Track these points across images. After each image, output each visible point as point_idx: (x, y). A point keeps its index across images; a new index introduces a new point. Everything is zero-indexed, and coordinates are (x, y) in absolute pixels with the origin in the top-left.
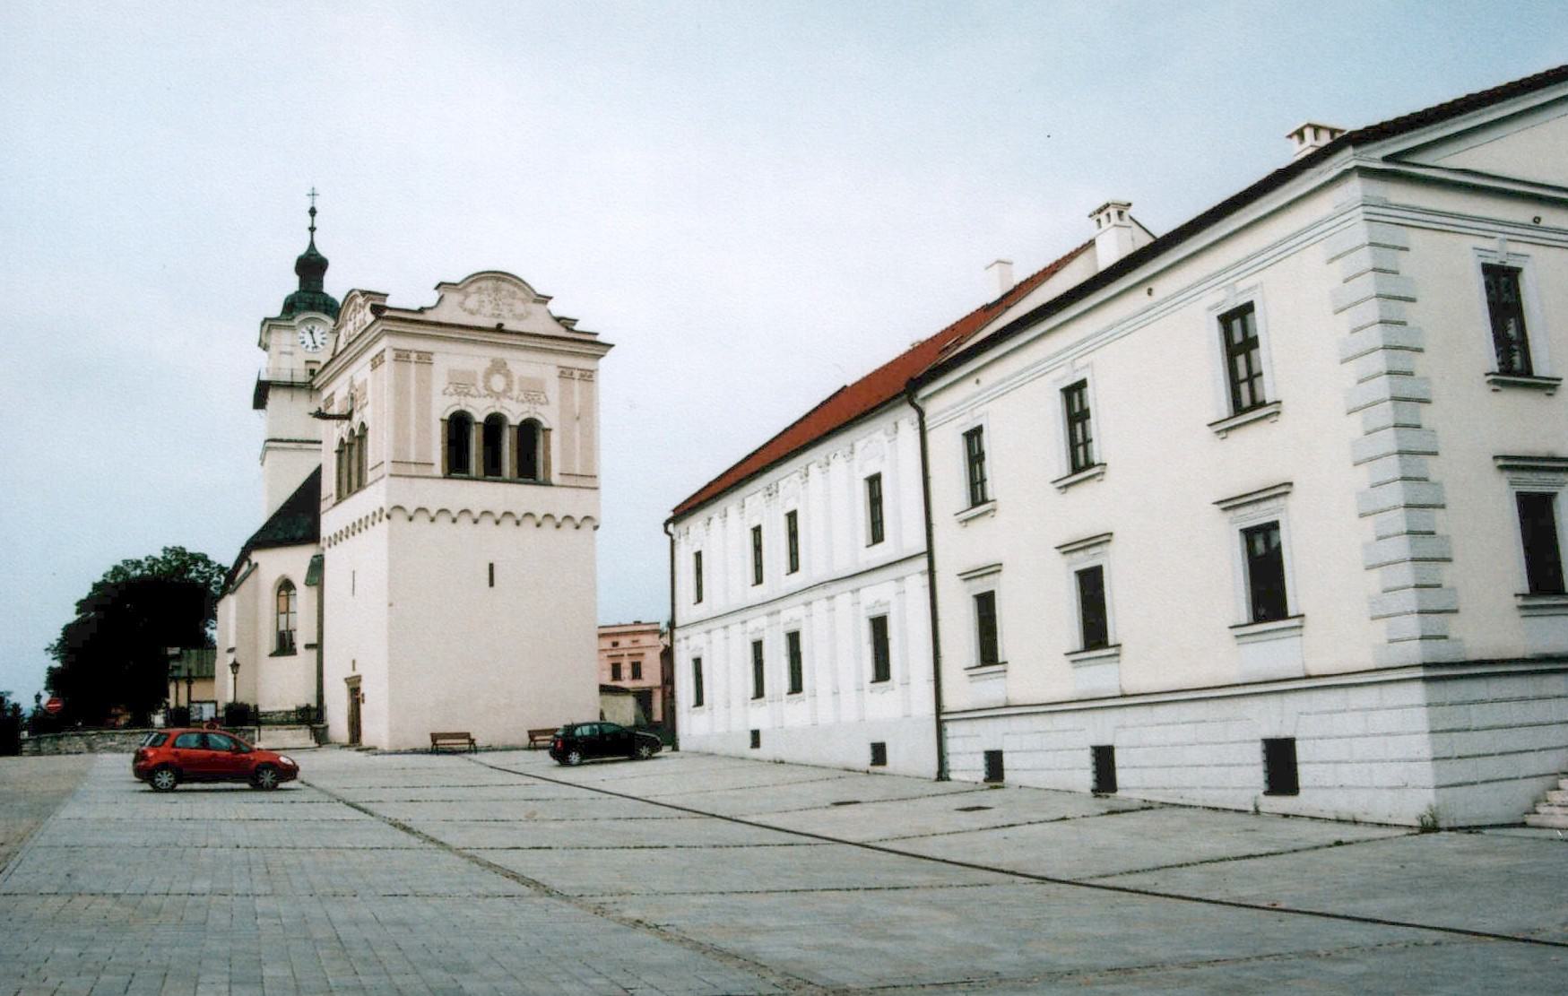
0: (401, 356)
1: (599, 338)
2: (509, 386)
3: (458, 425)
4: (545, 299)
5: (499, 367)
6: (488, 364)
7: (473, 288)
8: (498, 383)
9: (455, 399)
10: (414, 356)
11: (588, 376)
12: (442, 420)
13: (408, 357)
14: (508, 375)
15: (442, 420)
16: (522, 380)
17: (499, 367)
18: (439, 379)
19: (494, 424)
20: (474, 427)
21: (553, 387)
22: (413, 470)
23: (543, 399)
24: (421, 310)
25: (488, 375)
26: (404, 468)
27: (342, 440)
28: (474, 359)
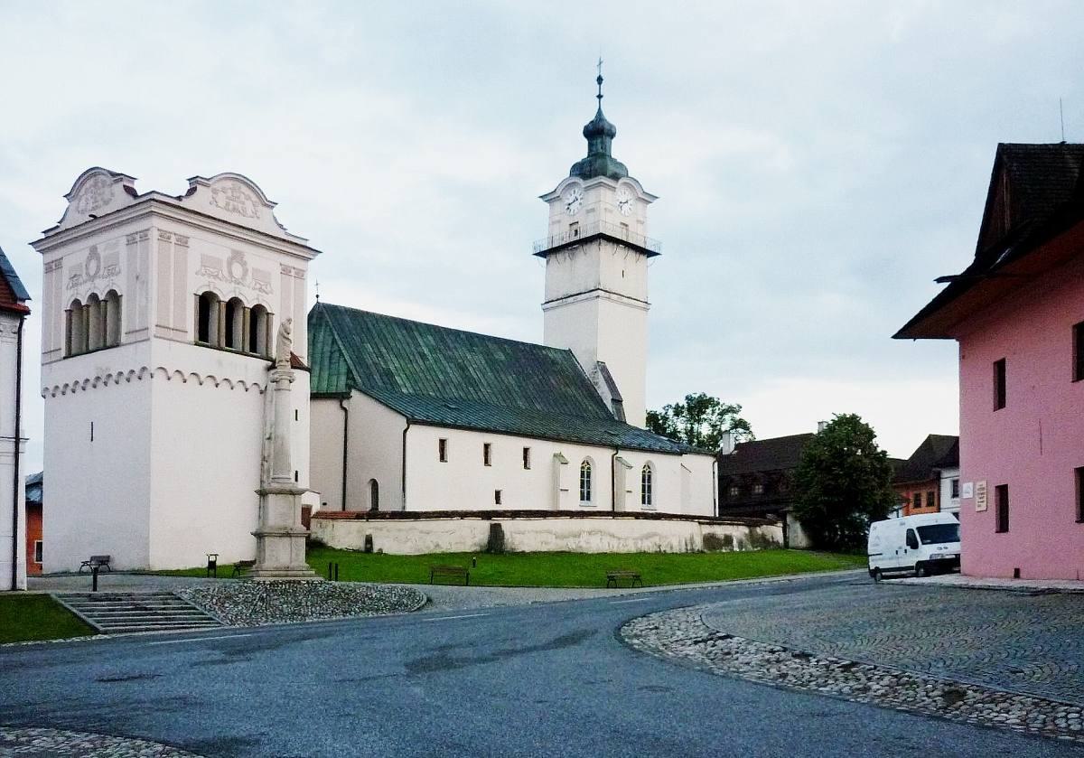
0: (164, 236)
1: (308, 244)
2: (245, 272)
3: (206, 301)
4: (271, 205)
5: (237, 256)
6: (229, 254)
7: (218, 186)
8: (237, 270)
9: (205, 280)
10: (173, 239)
11: (300, 275)
12: (195, 295)
13: (169, 238)
14: (244, 264)
15: (195, 295)
16: (255, 271)
17: (237, 256)
18: (193, 262)
19: (233, 305)
20: (216, 307)
21: (276, 278)
22: (172, 334)
23: (269, 289)
24: (179, 198)
25: (230, 264)
26: (169, 332)
27: (76, 302)
28: (219, 248)
